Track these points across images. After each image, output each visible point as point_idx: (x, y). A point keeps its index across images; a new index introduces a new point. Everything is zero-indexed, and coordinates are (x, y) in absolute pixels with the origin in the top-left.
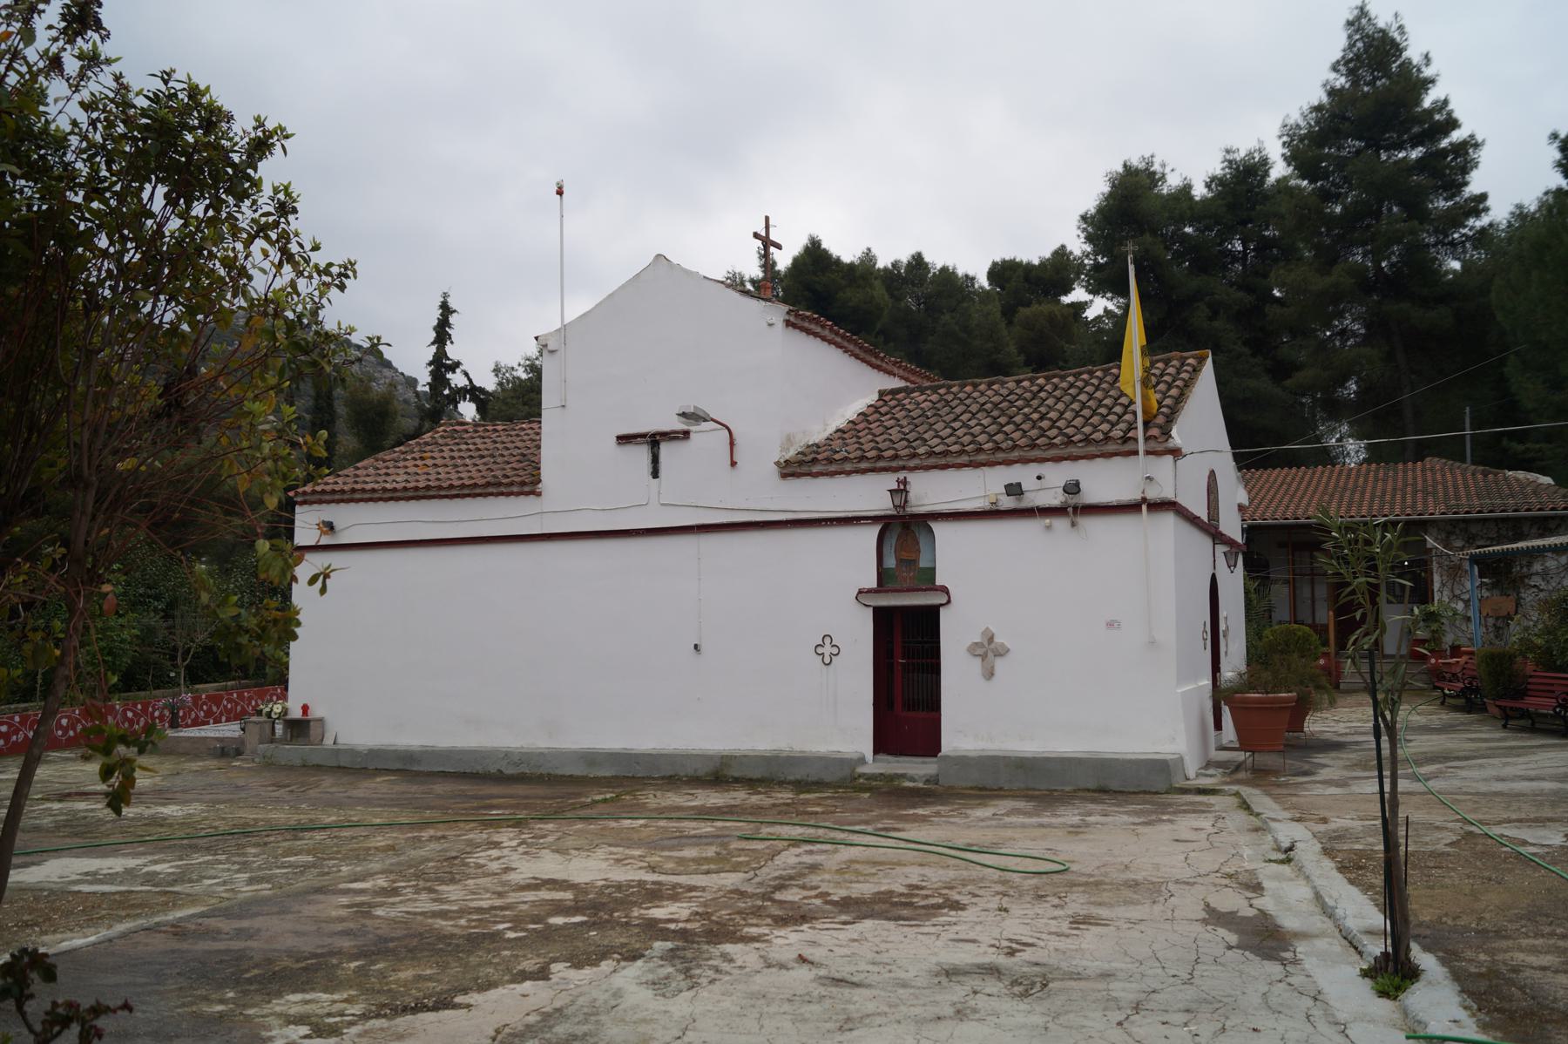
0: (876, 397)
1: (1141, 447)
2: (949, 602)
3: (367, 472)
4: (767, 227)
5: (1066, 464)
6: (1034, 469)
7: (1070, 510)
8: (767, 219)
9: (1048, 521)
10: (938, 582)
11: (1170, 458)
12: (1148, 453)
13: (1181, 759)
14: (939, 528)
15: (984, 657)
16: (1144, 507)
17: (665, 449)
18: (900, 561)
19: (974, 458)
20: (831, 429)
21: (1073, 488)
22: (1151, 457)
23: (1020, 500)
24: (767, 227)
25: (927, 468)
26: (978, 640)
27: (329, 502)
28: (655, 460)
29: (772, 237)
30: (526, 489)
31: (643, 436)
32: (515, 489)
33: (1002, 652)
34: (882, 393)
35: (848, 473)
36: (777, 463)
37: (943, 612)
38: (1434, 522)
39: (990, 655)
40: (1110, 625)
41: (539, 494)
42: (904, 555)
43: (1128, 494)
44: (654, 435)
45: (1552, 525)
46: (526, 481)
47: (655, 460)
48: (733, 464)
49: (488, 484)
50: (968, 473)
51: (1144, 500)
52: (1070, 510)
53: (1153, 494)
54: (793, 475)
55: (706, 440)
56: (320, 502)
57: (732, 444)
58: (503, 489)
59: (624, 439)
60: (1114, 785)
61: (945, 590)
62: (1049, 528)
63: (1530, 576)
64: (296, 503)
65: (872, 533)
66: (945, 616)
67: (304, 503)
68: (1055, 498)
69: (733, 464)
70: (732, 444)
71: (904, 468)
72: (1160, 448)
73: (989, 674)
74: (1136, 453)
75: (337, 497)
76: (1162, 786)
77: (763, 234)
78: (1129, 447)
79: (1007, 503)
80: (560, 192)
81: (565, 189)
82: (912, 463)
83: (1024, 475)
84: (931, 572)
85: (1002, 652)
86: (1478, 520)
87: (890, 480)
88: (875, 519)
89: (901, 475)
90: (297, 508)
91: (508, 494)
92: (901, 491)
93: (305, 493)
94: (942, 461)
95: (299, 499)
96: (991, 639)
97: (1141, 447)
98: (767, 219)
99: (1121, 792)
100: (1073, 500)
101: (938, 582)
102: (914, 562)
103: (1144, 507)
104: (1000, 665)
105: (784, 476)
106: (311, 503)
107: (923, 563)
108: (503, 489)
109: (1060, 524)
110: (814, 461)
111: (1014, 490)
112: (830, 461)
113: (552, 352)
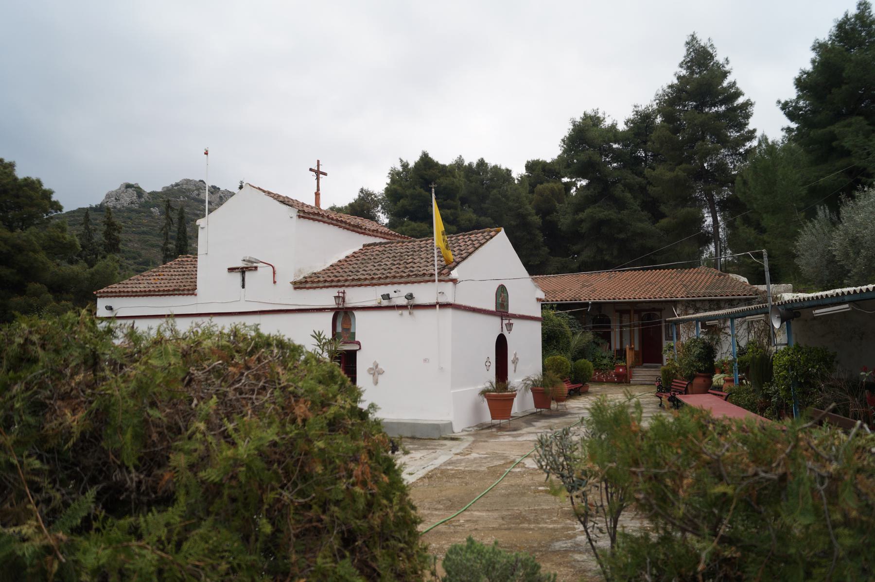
0: (361, 247)
1: (436, 278)
2: (360, 349)
3: (130, 284)
4: (318, 165)
5: (396, 285)
6: (396, 287)
7: (409, 307)
8: (318, 161)
9: (400, 312)
10: (357, 339)
11: (451, 283)
12: (440, 281)
13: (451, 424)
14: (357, 314)
15: (374, 374)
16: (438, 306)
17: (247, 274)
18: (343, 329)
19: (373, 282)
20: (328, 265)
21: (410, 297)
22: (443, 283)
23: (390, 302)
24: (318, 165)
25: (353, 286)
26: (372, 367)
27: (111, 297)
28: (243, 280)
29: (321, 170)
30: (191, 292)
31: (238, 268)
32: (186, 292)
33: (381, 373)
34: (364, 246)
35: (321, 288)
36: (291, 283)
37: (358, 353)
38: (682, 301)
39: (376, 374)
40: (425, 360)
41: (196, 295)
42: (345, 326)
43: (432, 300)
44: (242, 268)
45: (735, 303)
46: (190, 290)
47: (243, 280)
48: (275, 282)
49: (174, 290)
50: (370, 288)
51: (437, 303)
52: (409, 307)
53: (442, 300)
54: (298, 288)
55: (264, 272)
56: (107, 297)
57: (274, 273)
58: (181, 292)
59: (231, 270)
60: (418, 436)
61: (359, 343)
62: (401, 314)
63: (724, 328)
64: (97, 297)
65: (330, 316)
66: (359, 355)
67: (101, 297)
68: (403, 302)
69: (275, 282)
70: (274, 273)
71: (344, 286)
72: (447, 278)
73: (376, 383)
74: (434, 281)
75: (114, 294)
76: (437, 437)
77: (316, 169)
78: (432, 278)
79: (385, 303)
80: (206, 153)
81: (209, 153)
82: (347, 284)
83: (389, 290)
84: (353, 335)
85: (381, 373)
86: (700, 300)
87: (334, 292)
88: (332, 309)
89: (341, 290)
90: (99, 300)
91: (184, 295)
92: (341, 298)
93: (100, 292)
94: (359, 283)
95: (98, 295)
96: (377, 366)
97: (436, 278)
98: (318, 161)
99: (421, 439)
100: (412, 302)
101: (357, 339)
102: (349, 329)
103: (438, 306)
104: (381, 378)
105: (295, 288)
106: (104, 297)
107: (352, 331)
108: (181, 292)
109: (406, 313)
110: (306, 282)
111: (386, 297)
112: (313, 282)
113: (202, 228)
